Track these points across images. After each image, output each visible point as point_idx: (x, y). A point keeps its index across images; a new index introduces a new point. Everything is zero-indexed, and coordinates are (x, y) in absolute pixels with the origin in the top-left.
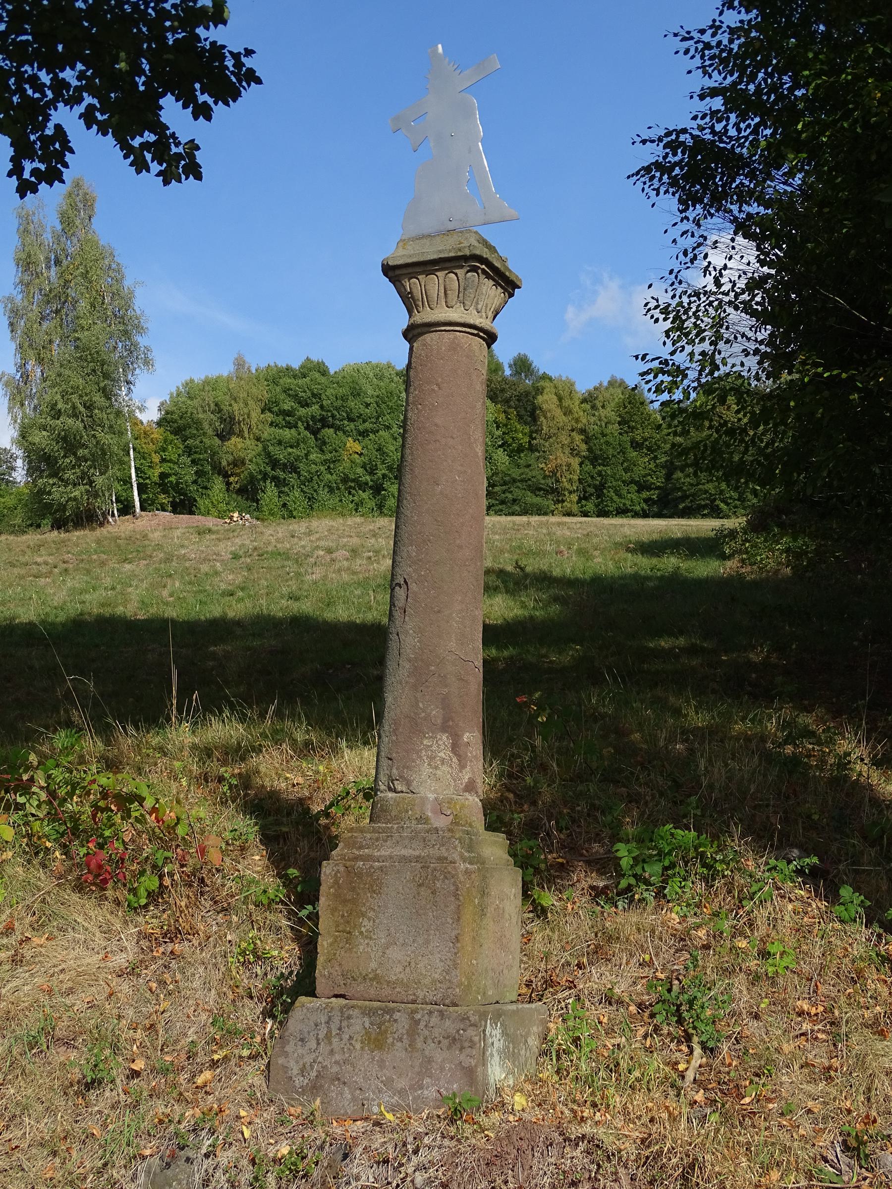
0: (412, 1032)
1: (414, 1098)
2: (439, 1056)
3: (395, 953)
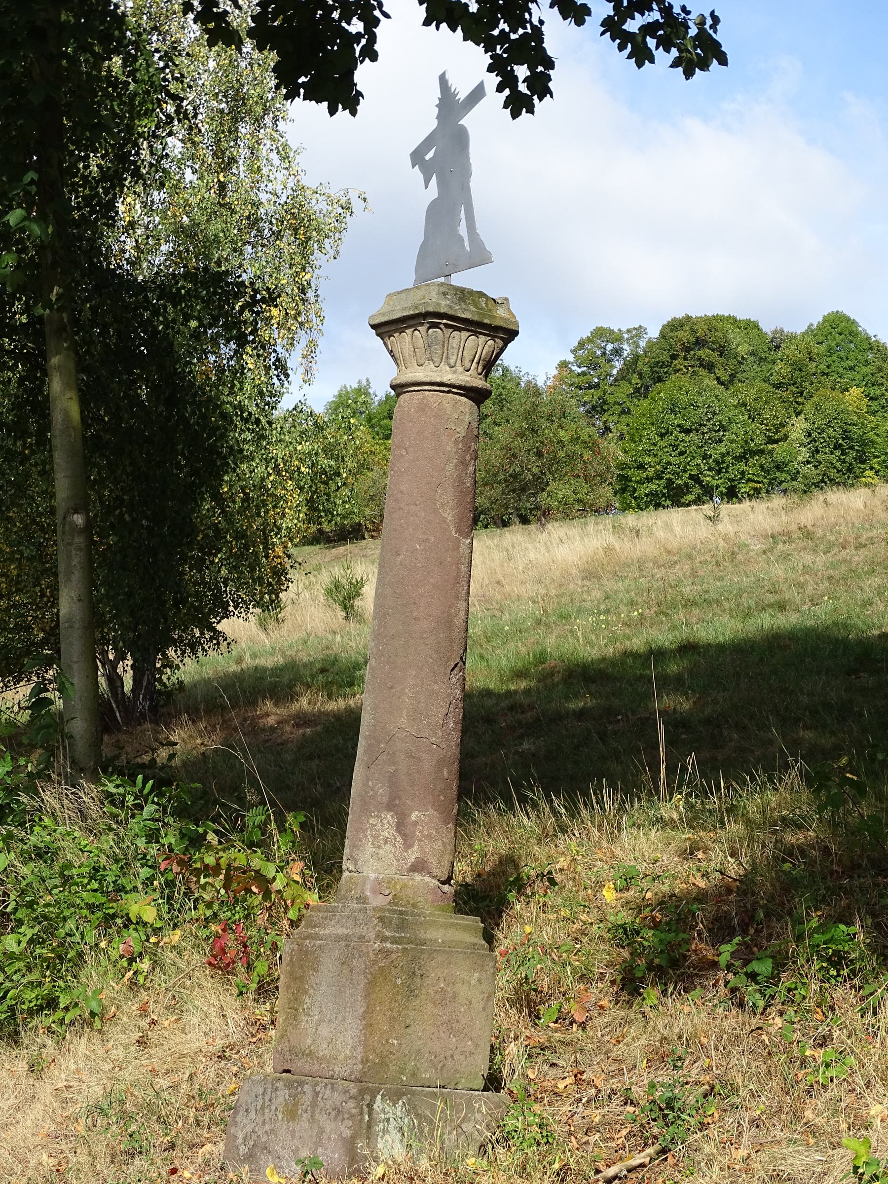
0: (314, 1105)
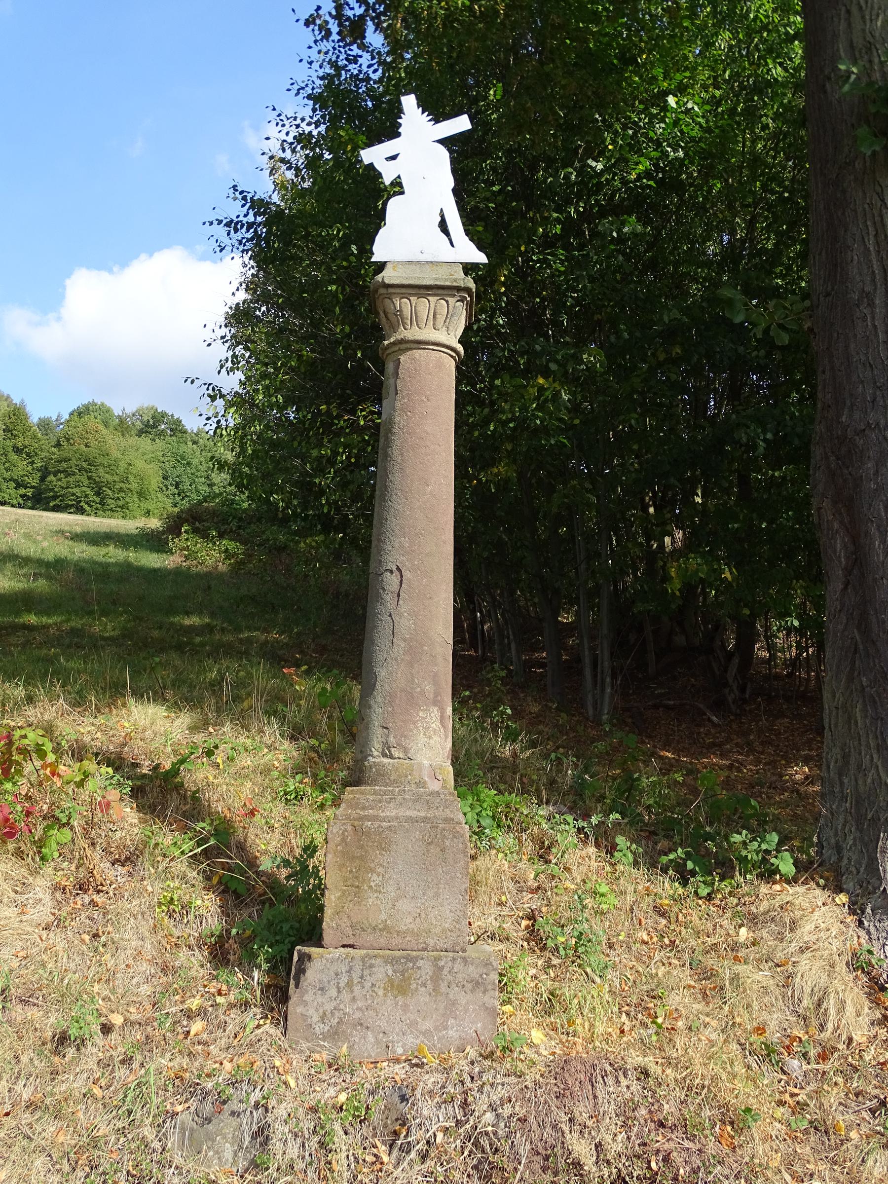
0: (436, 978)
1: (439, 1039)
2: (463, 999)
3: (404, 905)
